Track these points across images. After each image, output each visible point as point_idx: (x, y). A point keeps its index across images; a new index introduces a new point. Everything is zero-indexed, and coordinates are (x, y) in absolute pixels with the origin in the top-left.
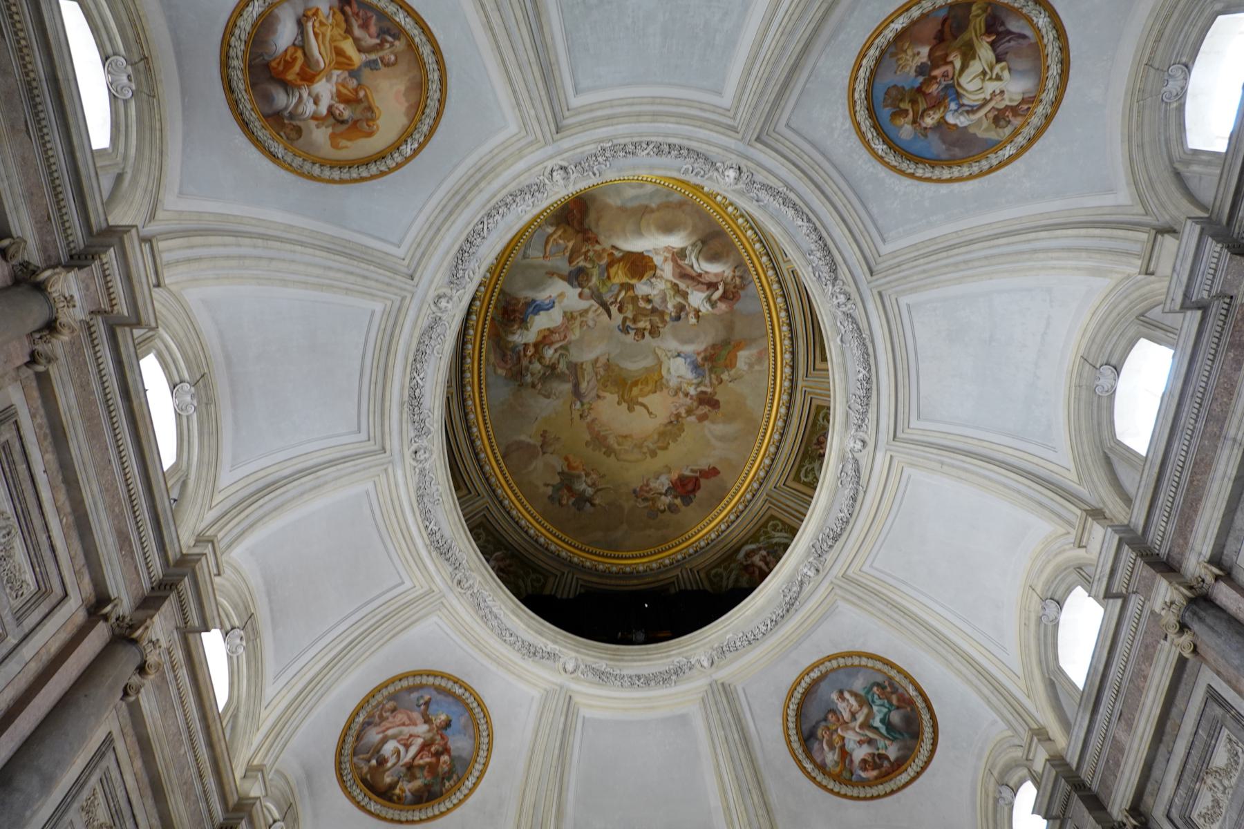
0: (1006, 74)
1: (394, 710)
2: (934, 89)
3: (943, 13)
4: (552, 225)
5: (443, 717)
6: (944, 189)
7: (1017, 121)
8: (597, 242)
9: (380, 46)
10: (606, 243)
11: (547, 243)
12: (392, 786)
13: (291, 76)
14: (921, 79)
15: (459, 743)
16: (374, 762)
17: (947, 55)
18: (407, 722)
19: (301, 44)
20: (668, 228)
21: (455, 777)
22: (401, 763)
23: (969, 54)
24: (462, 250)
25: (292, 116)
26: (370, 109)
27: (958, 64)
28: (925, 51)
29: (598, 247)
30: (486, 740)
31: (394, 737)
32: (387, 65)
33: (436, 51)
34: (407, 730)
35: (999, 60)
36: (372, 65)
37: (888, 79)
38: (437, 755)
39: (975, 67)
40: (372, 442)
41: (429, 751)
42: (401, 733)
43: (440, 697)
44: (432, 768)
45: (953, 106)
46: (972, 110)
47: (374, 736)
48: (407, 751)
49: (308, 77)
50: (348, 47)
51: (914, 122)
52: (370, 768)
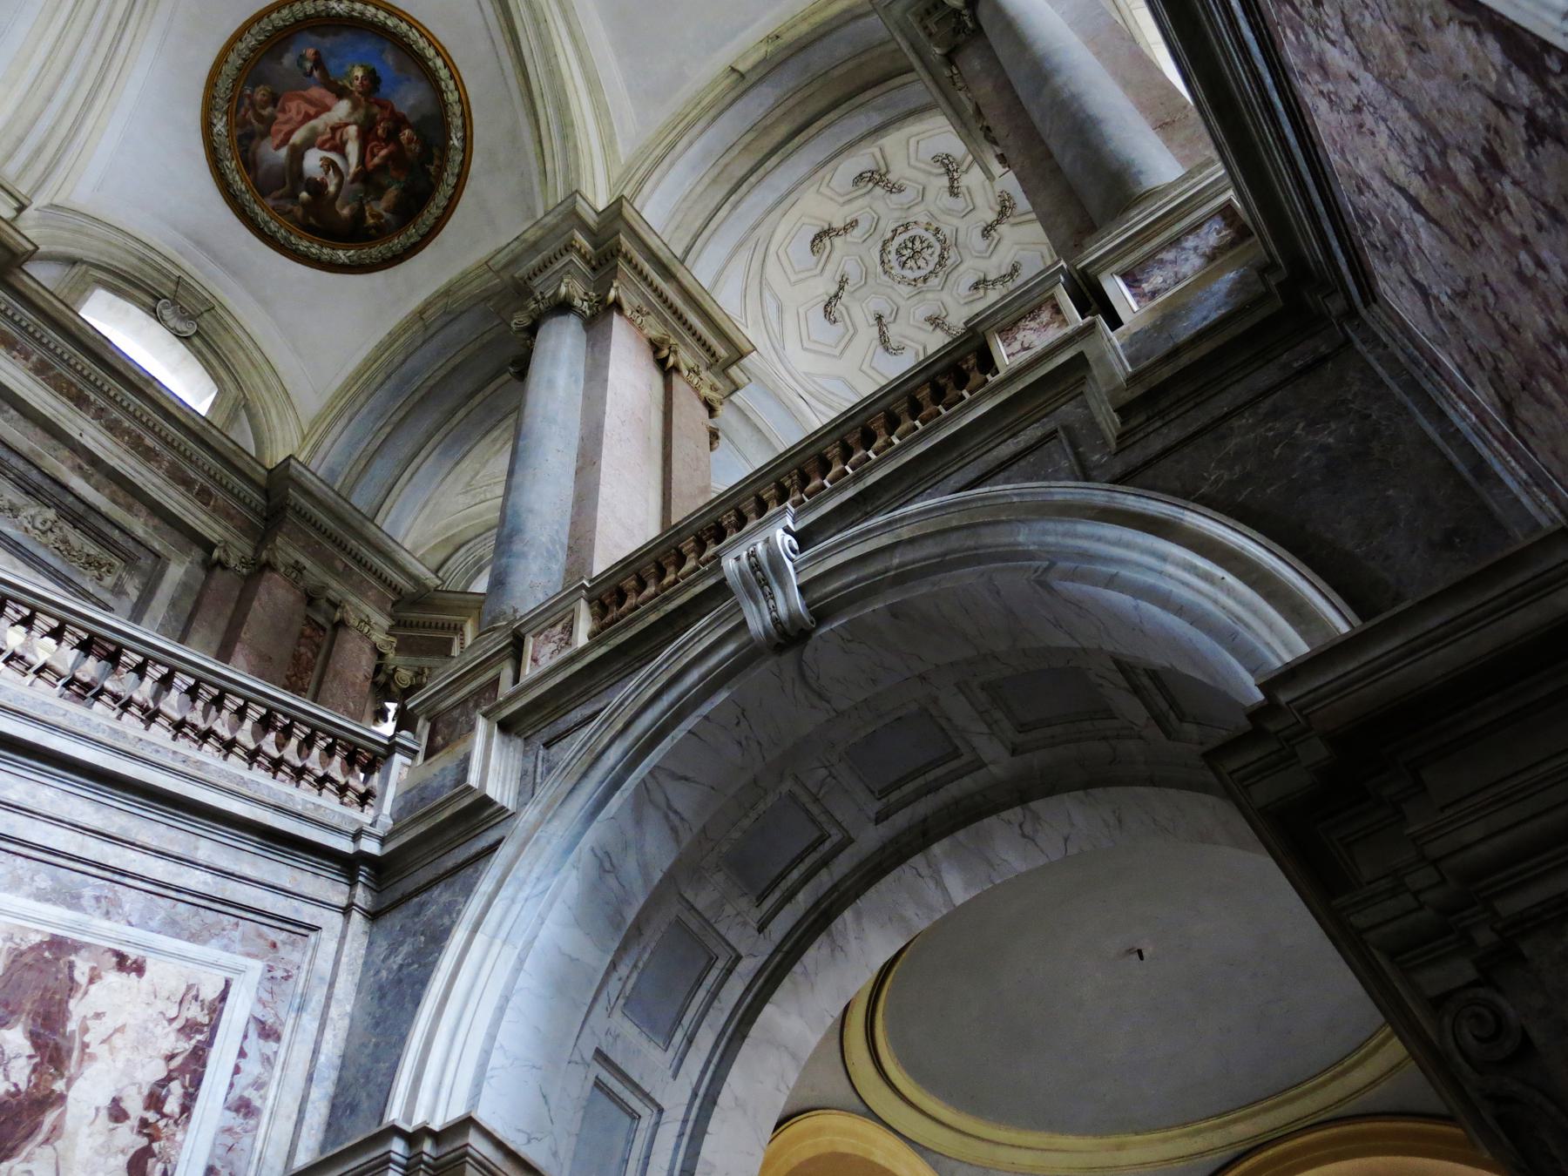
1: (274, 100)
5: (359, 73)
12: (358, 216)
15: (408, 98)
16: (304, 195)
18: (312, 111)
21: (436, 152)
22: (348, 179)
30: (439, 63)
31: (309, 143)
34: (322, 122)
38: (392, 136)
41: (378, 138)
42: (314, 134)
43: (328, 42)
44: (397, 159)
47: (274, 154)
48: (344, 156)
52: (304, 205)
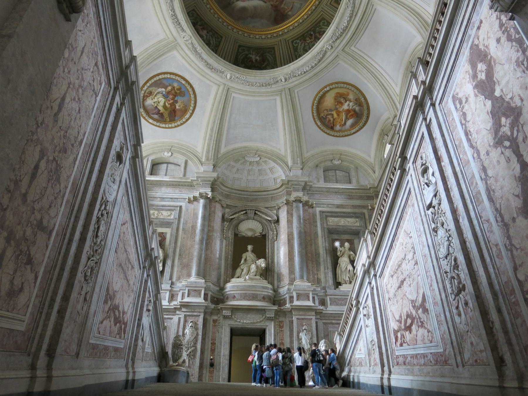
0: (153, 104)
2: (171, 97)
3: (176, 118)
4: (289, 15)
6: (159, 71)
7: (146, 94)
8: (272, 5)
9: (327, 115)
10: (269, 4)
11: (292, 8)
13: (352, 113)
14: (176, 99)
17: (171, 106)
19: (347, 119)
20: (244, 9)
23: (164, 107)
24: (319, 62)
25: (356, 104)
26: (335, 99)
27: (167, 104)
28: (177, 107)
29: (272, 3)
32: (327, 110)
33: (313, 113)
35: (156, 107)
36: (331, 110)
37: (185, 99)
39: (162, 104)
40: (373, 3)
45: (164, 93)
46: (158, 93)
49: (348, 111)
50: (335, 116)
51: (174, 87)
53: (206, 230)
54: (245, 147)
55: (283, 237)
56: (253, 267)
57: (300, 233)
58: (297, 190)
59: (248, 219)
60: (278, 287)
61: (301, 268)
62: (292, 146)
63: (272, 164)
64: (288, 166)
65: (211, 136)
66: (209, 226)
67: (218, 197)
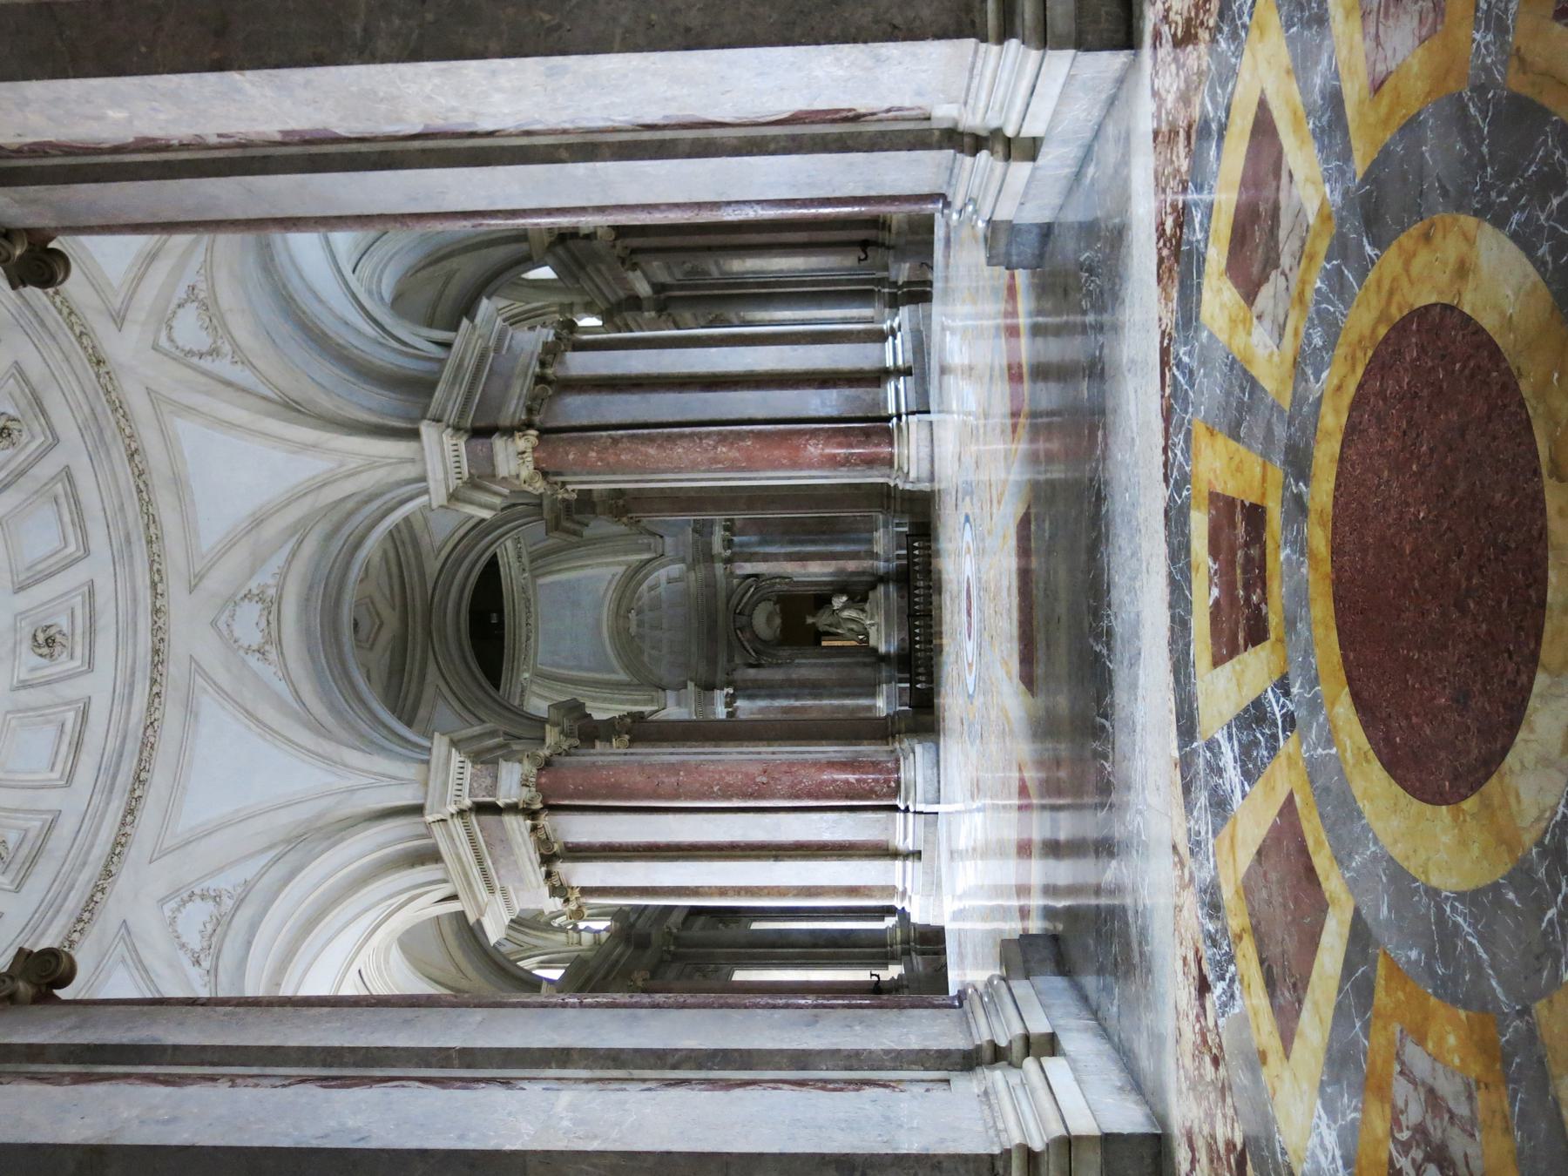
53: (794, 691)
54: (611, 637)
55: (790, 568)
56: (846, 614)
57: (792, 543)
58: (709, 545)
59: (751, 625)
60: (873, 574)
61: (854, 542)
62: (615, 553)
63: (645, 586)
64: (649, 561)
65: (605, 700)
66: (781, 687)
67: (721, 677)
